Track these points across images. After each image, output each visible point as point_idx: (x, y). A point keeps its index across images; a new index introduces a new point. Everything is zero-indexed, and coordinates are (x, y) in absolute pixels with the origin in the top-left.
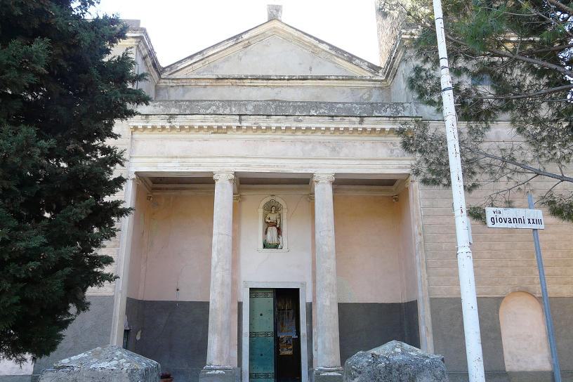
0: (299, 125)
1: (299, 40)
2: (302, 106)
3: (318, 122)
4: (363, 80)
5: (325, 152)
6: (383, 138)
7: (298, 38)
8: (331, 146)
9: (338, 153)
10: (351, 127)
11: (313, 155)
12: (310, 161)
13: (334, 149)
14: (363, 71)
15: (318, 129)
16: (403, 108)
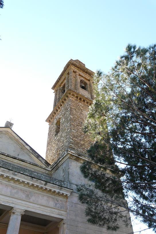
0: (14, 177)
1: (17, 141)
2: (17, 168)
3: (24, 178)
4: (41, 168)
5: (23, 196)
6: (53, 196)
7: (17, 139)
8: (27, 194)
9: (30, 199)
10: (40, 186)
11: (16, 196)
12: (14, 199)
13: (28, 196)
14: (42, 164)
15: (23, 182)
16: (64, 184)
